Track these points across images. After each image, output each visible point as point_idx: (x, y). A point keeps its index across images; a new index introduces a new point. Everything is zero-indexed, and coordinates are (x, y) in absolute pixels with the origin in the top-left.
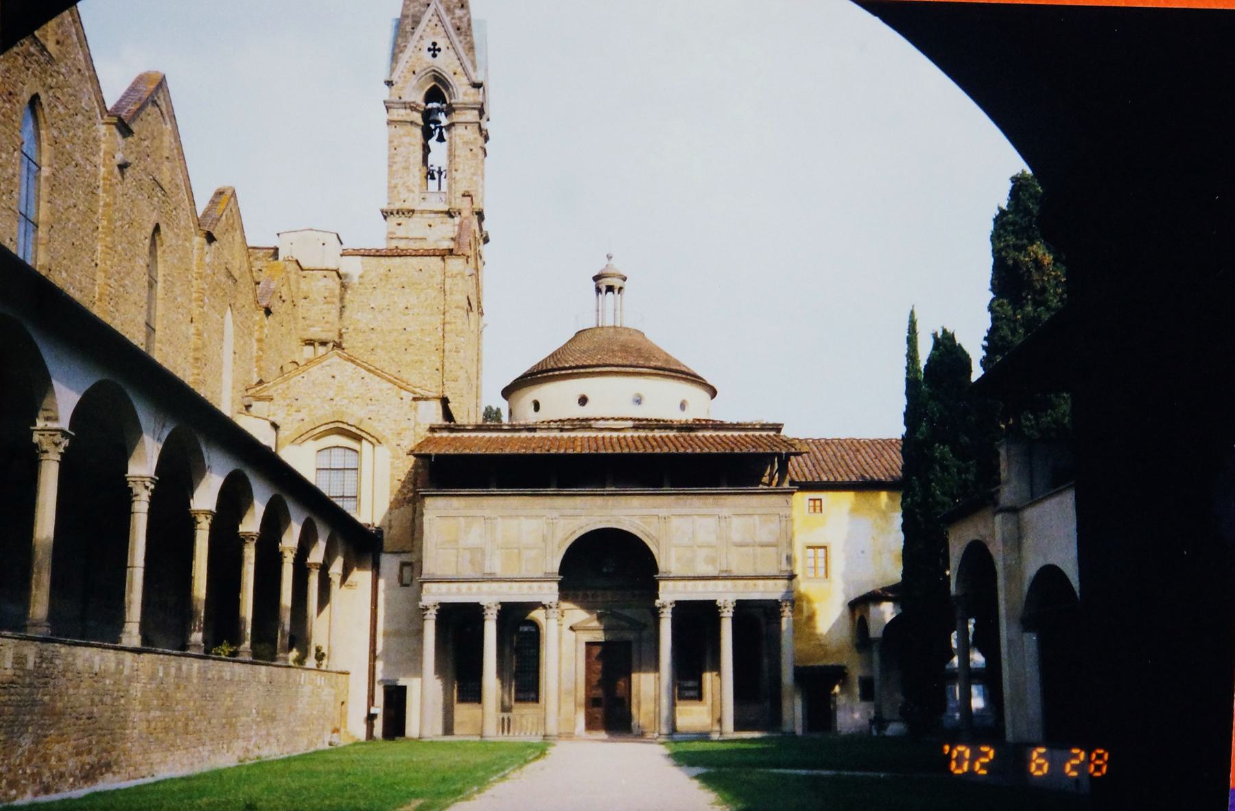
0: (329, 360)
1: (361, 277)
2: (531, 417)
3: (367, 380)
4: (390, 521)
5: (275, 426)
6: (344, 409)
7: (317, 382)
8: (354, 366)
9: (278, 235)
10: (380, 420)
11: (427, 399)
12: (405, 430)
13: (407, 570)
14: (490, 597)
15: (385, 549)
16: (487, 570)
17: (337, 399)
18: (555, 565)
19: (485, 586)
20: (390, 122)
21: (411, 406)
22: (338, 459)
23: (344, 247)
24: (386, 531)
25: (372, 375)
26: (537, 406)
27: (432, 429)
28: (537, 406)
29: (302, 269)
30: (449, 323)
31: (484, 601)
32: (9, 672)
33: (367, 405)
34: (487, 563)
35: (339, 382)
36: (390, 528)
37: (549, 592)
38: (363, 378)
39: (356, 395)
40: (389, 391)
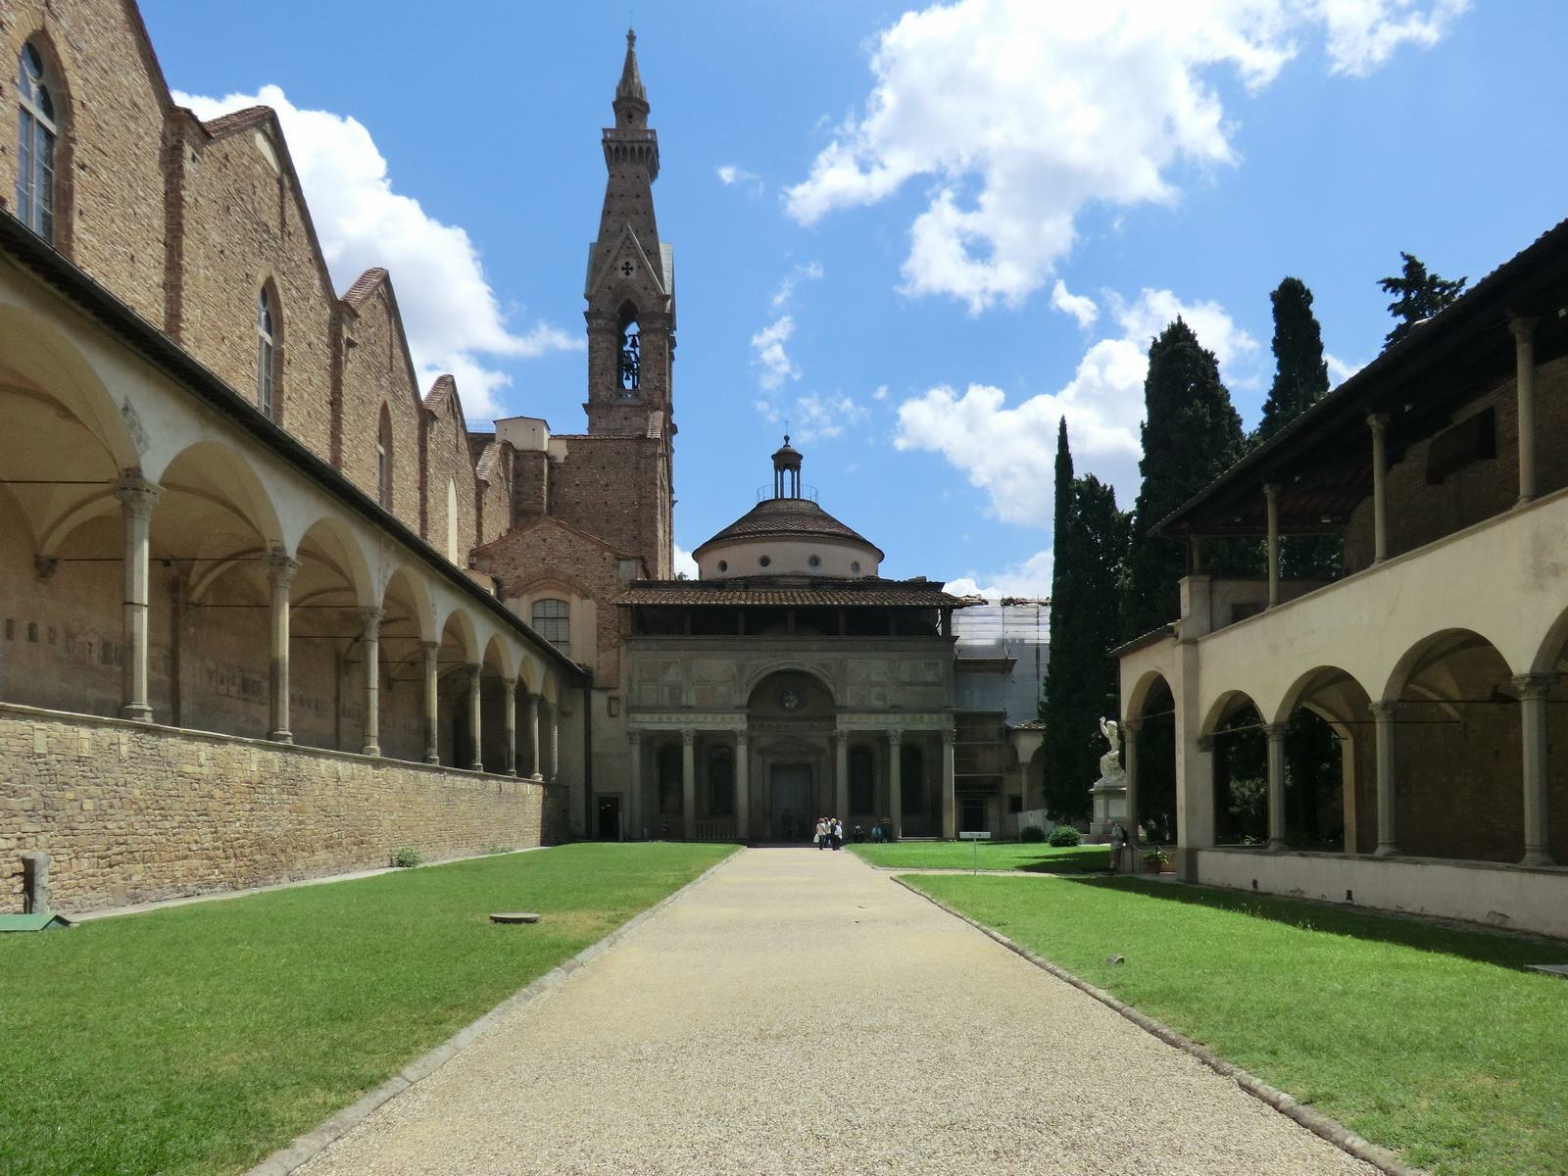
0: (541, 526)
1: (566, 458)
2: (719, 575)
3: (574, 543)
4: (598, 662)
5: (497, 582)
6: (554, 567)
7: (531, 544)
9: (494, 422)
11: (628, 559)
12: (609, 585)
13: (613, 702)
14: (686, 724)
15: (594, 686)
16: (684, 702)
18: (743, 699)
19: (683, 717)
20: (590, 331)
22: (552, 612)
23: (554, 433)
24: (595, 669)
26: (723, 566)
27: (635, 585)
28: (723, 566)
29: (516, 451)
30: (646, 498)
31: (683, 727)
32: (257, 774)
33: (575, 564)
34: (684, 698)
35: (550, 544)
36: (598, 668)
37: (738, 723)
38: (570, 541)
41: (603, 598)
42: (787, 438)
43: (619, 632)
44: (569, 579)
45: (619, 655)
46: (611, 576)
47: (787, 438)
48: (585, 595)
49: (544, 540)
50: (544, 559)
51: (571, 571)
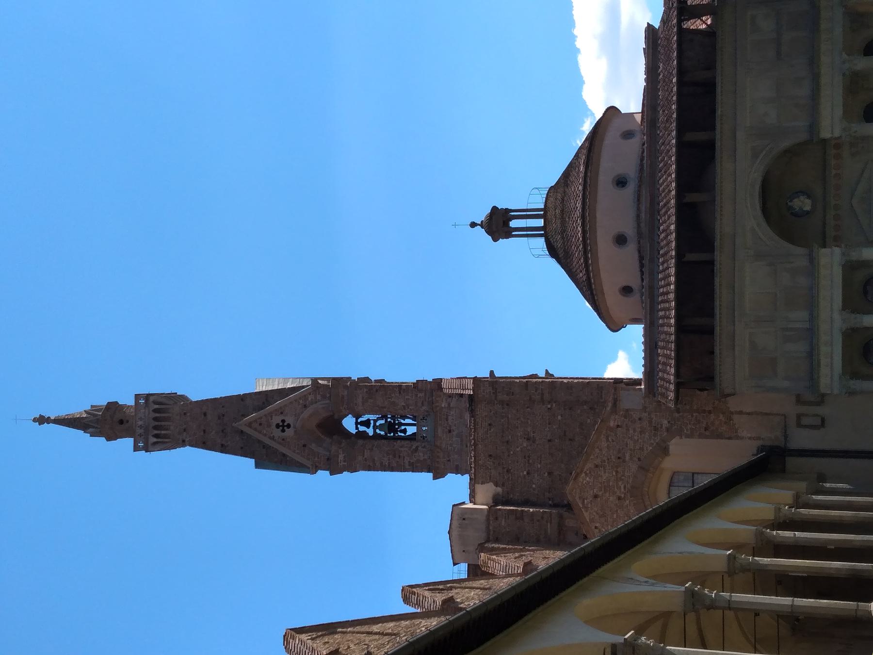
0: (578, 500)
3: (598, 461)
6: (629, 486)
7: (602, 513)
8: (583, 475)
10: (642, 449)
12: (650, 422)
17: (618, 494)
21: (625, 417)
25: (592, 457)
33: (624, 461)
39: (614, 474)
40: (610, 440)
41: (668, 430)
42: (473, 225)
43: (710, 412)
44: (643, 469)
45: (741, 413)
46: (640, 419)
47: (473, 225)
48: (665, 451)
49: (596, 496)
50: (619, 498)
51: (634, 467)
